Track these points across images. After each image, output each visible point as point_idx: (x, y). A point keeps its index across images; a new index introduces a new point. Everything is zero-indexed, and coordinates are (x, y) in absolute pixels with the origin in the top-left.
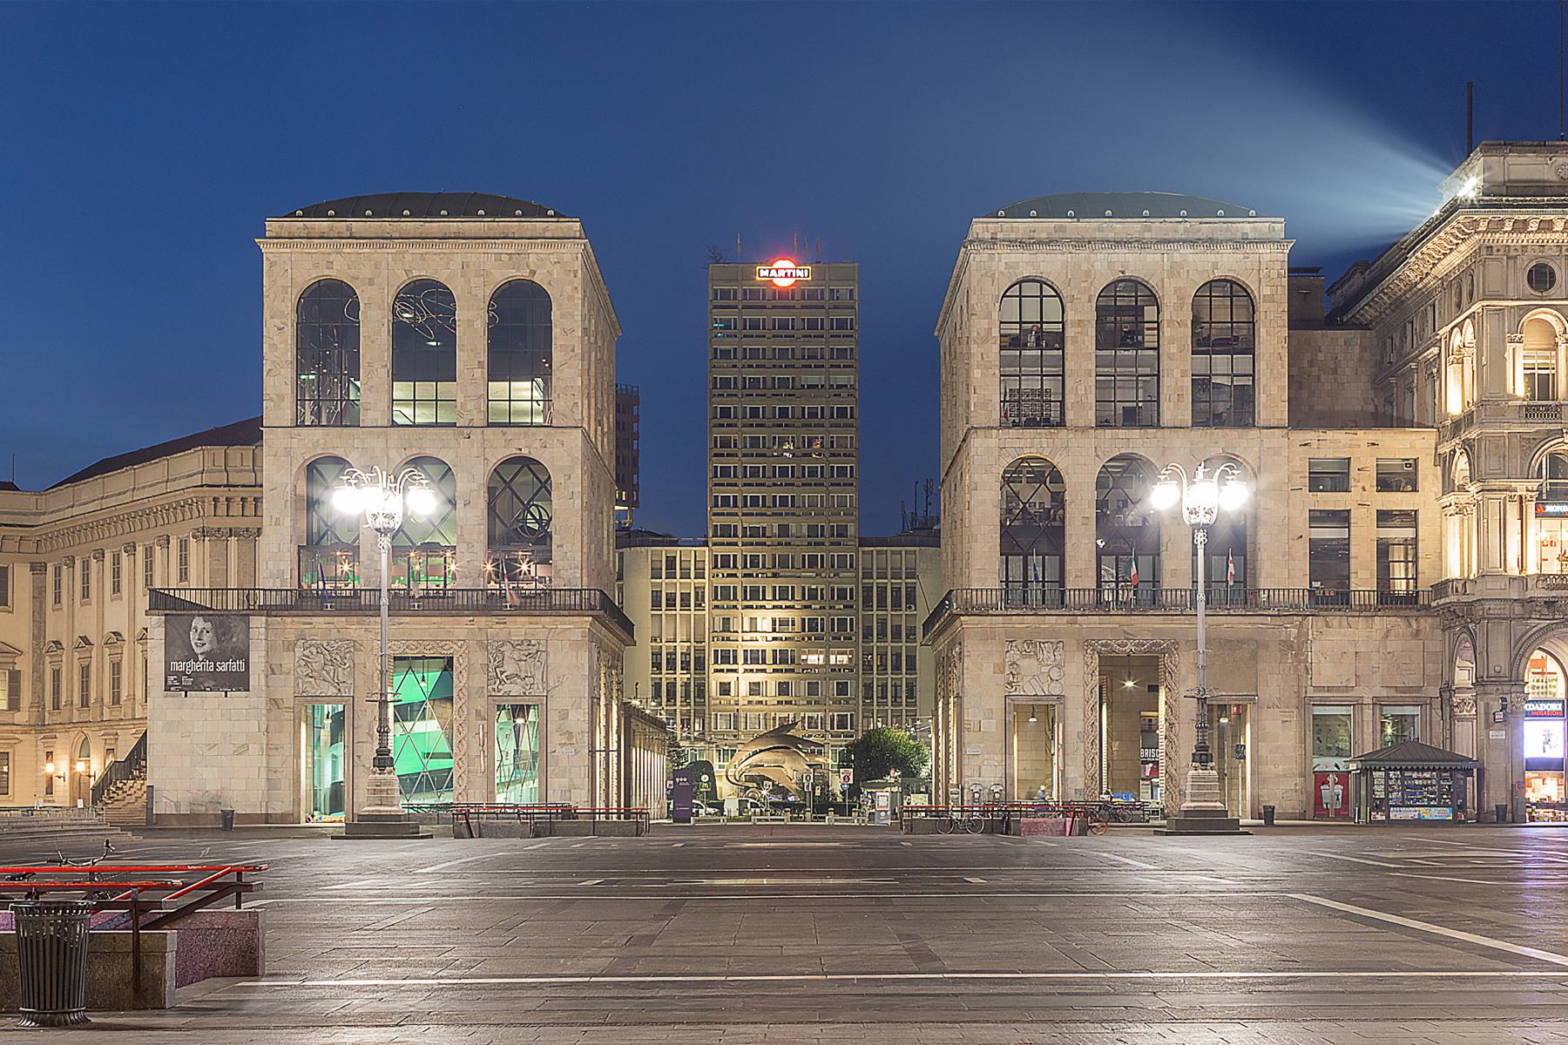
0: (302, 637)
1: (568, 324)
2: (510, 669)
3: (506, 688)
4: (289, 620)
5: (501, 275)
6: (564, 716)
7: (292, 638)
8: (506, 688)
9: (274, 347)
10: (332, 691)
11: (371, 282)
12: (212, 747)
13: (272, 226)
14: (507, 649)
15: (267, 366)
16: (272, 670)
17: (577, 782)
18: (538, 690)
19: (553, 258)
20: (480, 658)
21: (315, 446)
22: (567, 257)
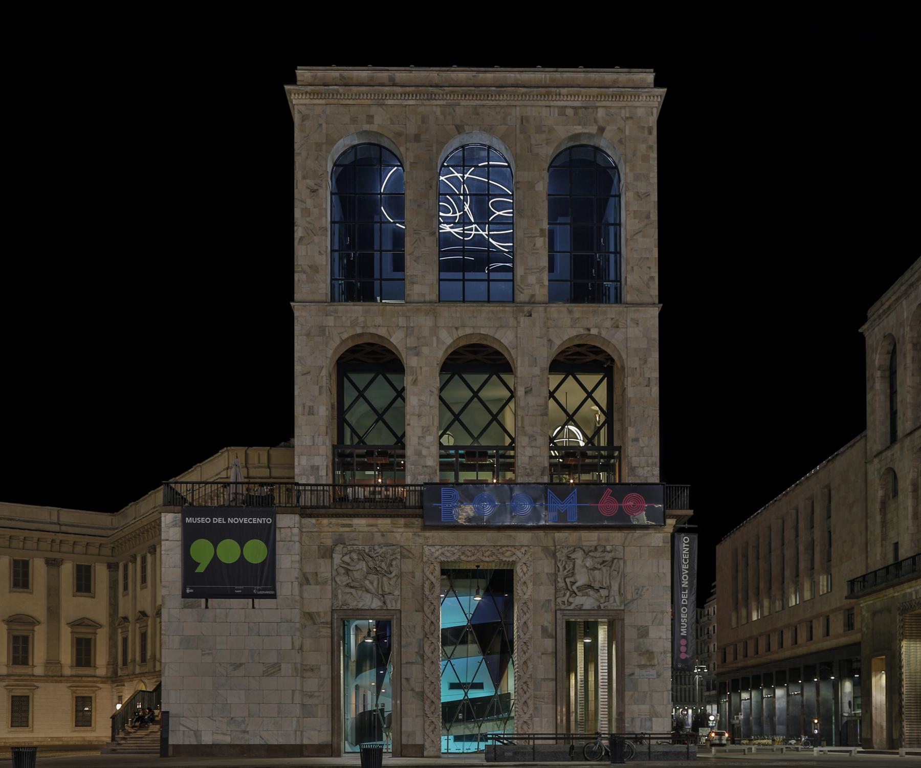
0: (340, 540)
1: (642, 187)
2: (582, 579)
3: (579, 600)
4: (325, 521)
5: (564, 132)
6: (643, 632)
7: (329, 542)
8: (579, 600)
9: (306, 212)
10: (376, 604)
11: (417, 138)
12: (237, 666)
13: (303, 73)
14: (579, 555)
15: (299, 233)
16: (305, 580)
17: (659, 709)
18: (615, 603)
19: (625, 113)
20: (546, 566)
21: (354, 325)
22: (640, 112)
